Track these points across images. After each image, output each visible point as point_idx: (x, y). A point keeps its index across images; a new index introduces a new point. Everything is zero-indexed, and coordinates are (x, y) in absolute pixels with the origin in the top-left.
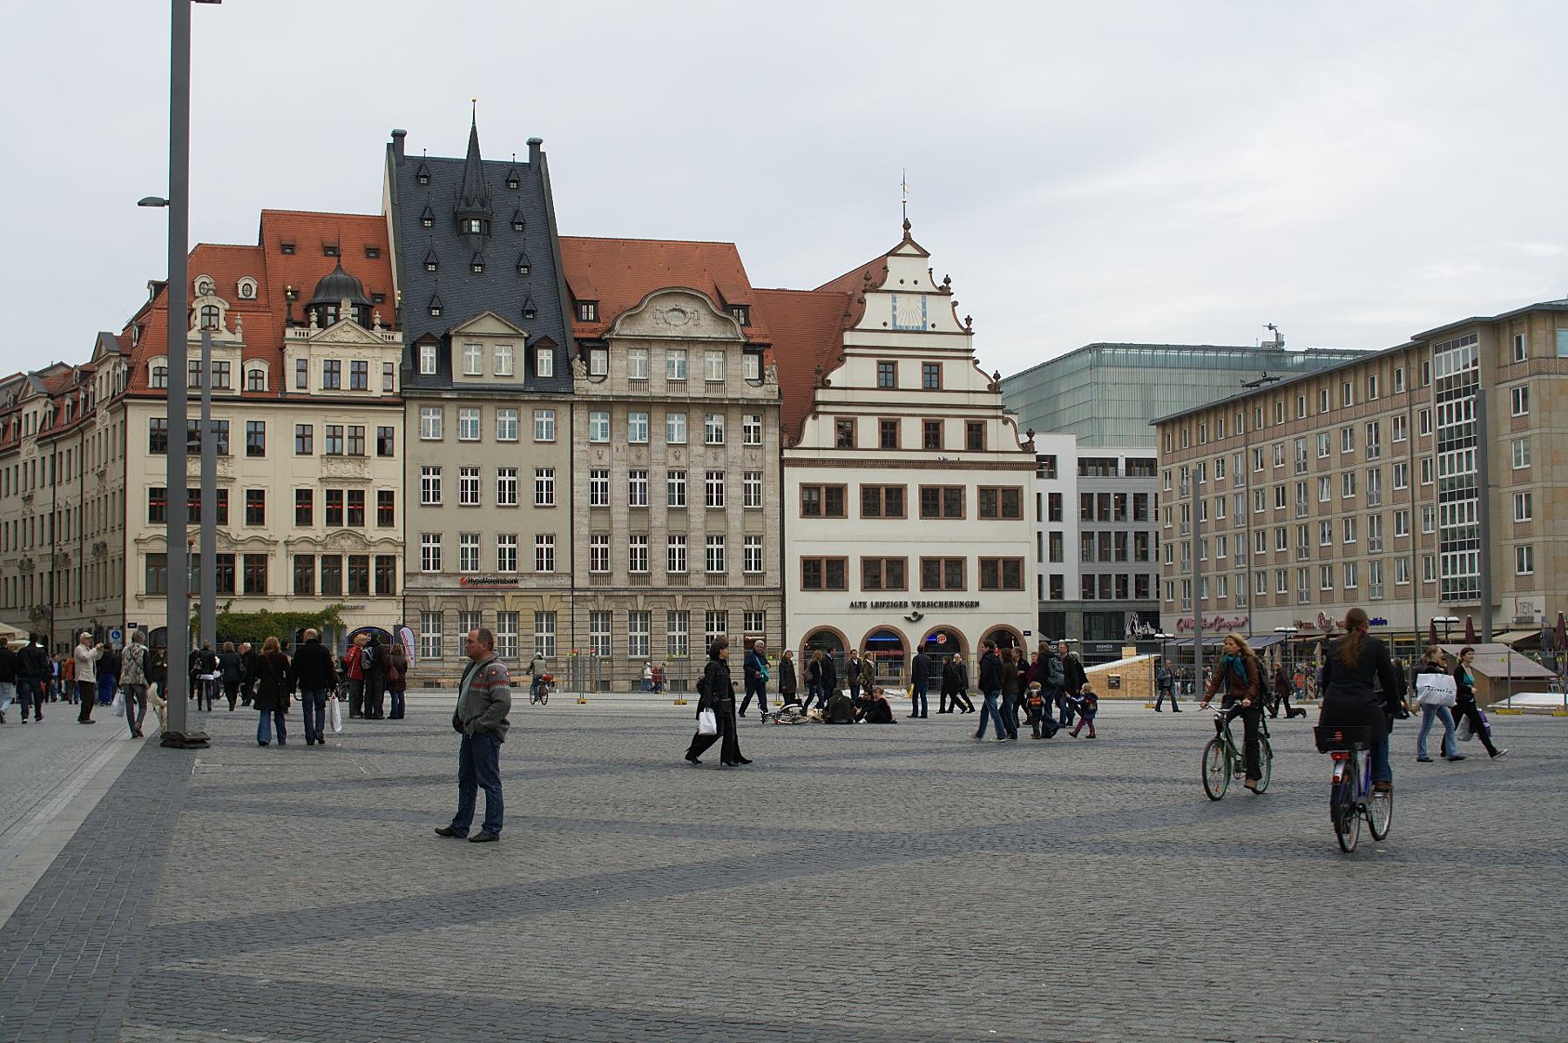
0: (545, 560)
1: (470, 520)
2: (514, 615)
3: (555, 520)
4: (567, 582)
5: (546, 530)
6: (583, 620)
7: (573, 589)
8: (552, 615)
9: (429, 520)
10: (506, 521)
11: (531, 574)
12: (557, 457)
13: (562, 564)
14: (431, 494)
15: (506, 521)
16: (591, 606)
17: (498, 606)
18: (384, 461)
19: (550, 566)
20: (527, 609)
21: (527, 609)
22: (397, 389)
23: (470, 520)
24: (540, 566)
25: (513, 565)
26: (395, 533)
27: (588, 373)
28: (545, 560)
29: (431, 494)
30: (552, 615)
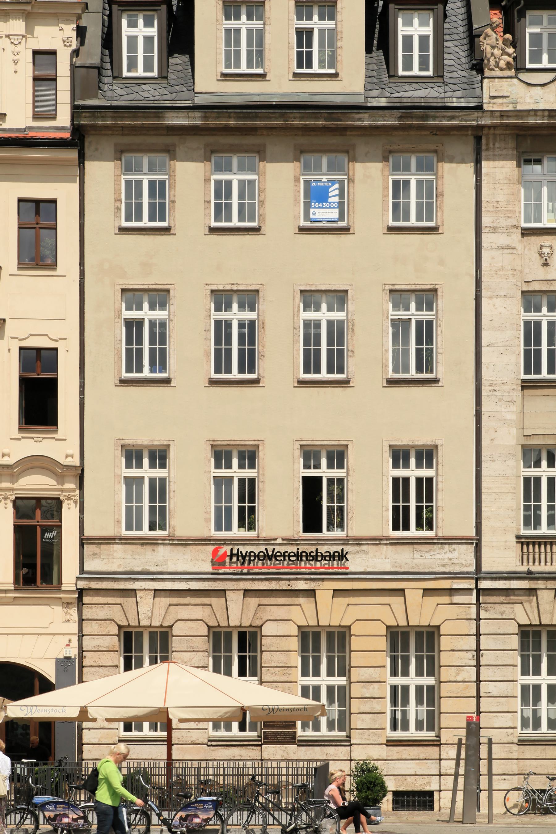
0: (414, 505)
1: (236, 415)
2: (340, 638)
3: (434, 415)
4: (463, 558)
5: (415, 436)
6: (502, 648)
7: (478, 574)
8: (429, 637)
9: (141, 416)
10: (323, 416)
11: (377, 541)
12: (441, 261)
13: (452, 512)
14: (145, 353)
15: (323, 416)
16: (523, 614)
17: (301, 613)
18: (37, 281)
19: (426, 521)
20: (369, 623)
21: (369, 623)
22: (64, 118)
23: (236, 415)
24: (400, 520)
25: (339, 518)
26: (59, 445)
27: (518, 66)
28: (414, 505)
29: (145, 353)
30: (429, 637)
